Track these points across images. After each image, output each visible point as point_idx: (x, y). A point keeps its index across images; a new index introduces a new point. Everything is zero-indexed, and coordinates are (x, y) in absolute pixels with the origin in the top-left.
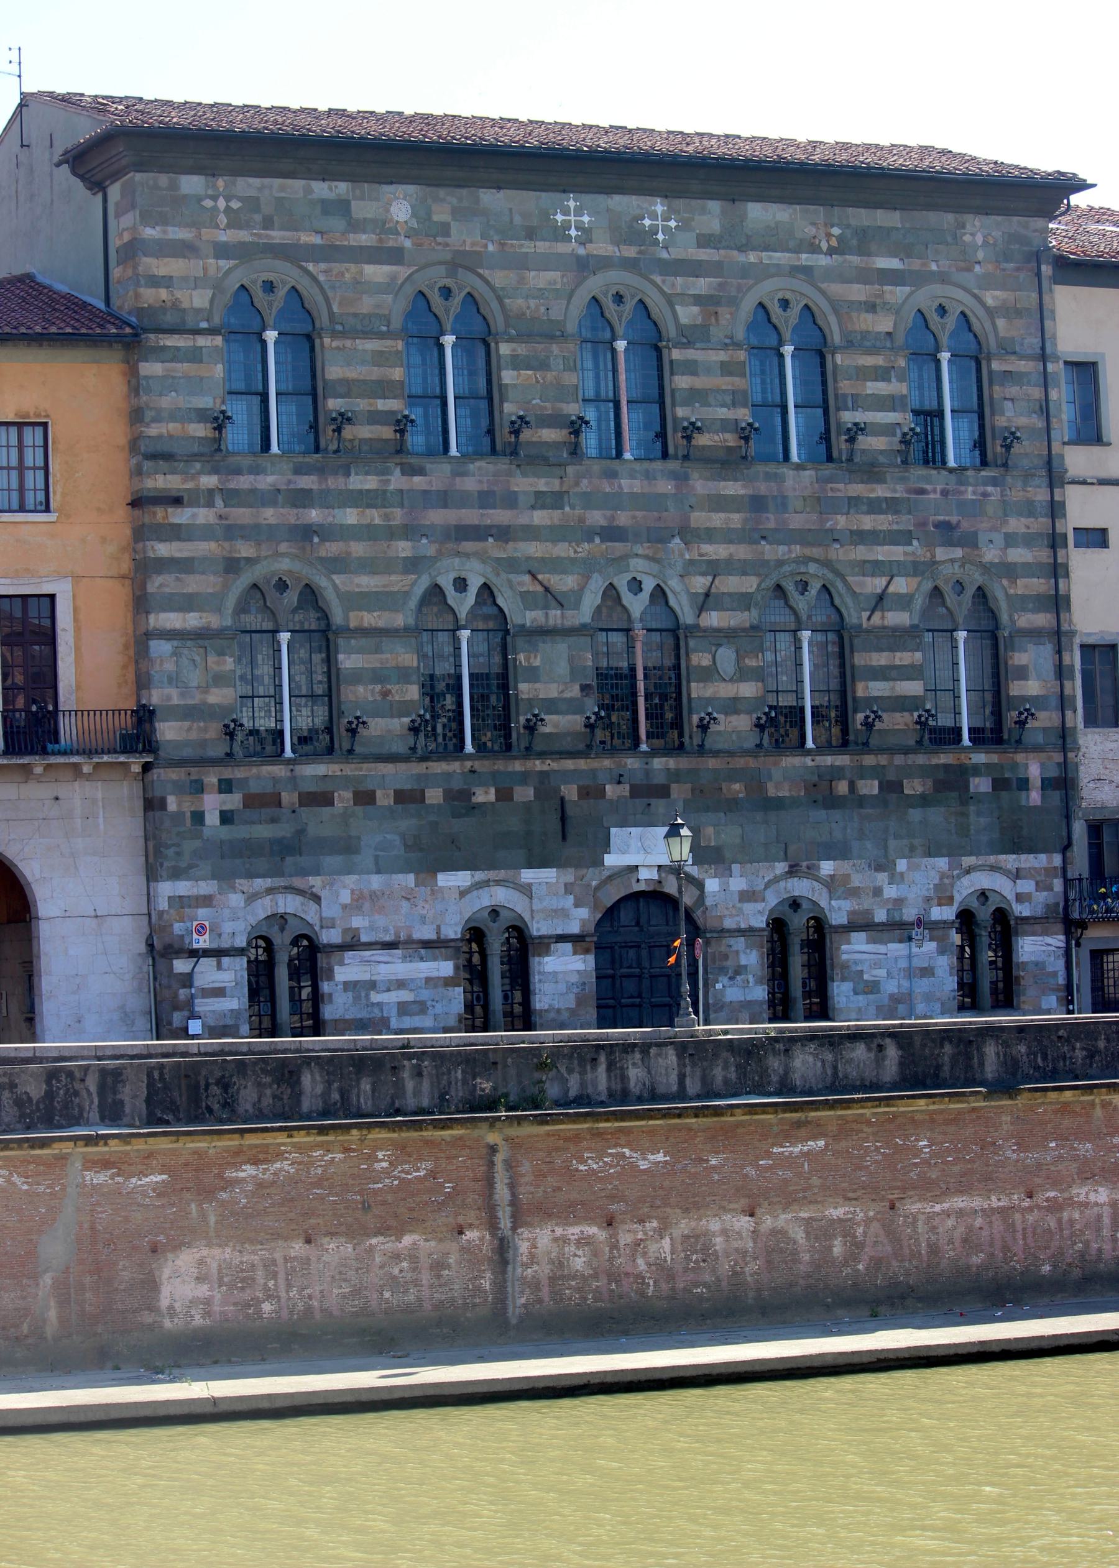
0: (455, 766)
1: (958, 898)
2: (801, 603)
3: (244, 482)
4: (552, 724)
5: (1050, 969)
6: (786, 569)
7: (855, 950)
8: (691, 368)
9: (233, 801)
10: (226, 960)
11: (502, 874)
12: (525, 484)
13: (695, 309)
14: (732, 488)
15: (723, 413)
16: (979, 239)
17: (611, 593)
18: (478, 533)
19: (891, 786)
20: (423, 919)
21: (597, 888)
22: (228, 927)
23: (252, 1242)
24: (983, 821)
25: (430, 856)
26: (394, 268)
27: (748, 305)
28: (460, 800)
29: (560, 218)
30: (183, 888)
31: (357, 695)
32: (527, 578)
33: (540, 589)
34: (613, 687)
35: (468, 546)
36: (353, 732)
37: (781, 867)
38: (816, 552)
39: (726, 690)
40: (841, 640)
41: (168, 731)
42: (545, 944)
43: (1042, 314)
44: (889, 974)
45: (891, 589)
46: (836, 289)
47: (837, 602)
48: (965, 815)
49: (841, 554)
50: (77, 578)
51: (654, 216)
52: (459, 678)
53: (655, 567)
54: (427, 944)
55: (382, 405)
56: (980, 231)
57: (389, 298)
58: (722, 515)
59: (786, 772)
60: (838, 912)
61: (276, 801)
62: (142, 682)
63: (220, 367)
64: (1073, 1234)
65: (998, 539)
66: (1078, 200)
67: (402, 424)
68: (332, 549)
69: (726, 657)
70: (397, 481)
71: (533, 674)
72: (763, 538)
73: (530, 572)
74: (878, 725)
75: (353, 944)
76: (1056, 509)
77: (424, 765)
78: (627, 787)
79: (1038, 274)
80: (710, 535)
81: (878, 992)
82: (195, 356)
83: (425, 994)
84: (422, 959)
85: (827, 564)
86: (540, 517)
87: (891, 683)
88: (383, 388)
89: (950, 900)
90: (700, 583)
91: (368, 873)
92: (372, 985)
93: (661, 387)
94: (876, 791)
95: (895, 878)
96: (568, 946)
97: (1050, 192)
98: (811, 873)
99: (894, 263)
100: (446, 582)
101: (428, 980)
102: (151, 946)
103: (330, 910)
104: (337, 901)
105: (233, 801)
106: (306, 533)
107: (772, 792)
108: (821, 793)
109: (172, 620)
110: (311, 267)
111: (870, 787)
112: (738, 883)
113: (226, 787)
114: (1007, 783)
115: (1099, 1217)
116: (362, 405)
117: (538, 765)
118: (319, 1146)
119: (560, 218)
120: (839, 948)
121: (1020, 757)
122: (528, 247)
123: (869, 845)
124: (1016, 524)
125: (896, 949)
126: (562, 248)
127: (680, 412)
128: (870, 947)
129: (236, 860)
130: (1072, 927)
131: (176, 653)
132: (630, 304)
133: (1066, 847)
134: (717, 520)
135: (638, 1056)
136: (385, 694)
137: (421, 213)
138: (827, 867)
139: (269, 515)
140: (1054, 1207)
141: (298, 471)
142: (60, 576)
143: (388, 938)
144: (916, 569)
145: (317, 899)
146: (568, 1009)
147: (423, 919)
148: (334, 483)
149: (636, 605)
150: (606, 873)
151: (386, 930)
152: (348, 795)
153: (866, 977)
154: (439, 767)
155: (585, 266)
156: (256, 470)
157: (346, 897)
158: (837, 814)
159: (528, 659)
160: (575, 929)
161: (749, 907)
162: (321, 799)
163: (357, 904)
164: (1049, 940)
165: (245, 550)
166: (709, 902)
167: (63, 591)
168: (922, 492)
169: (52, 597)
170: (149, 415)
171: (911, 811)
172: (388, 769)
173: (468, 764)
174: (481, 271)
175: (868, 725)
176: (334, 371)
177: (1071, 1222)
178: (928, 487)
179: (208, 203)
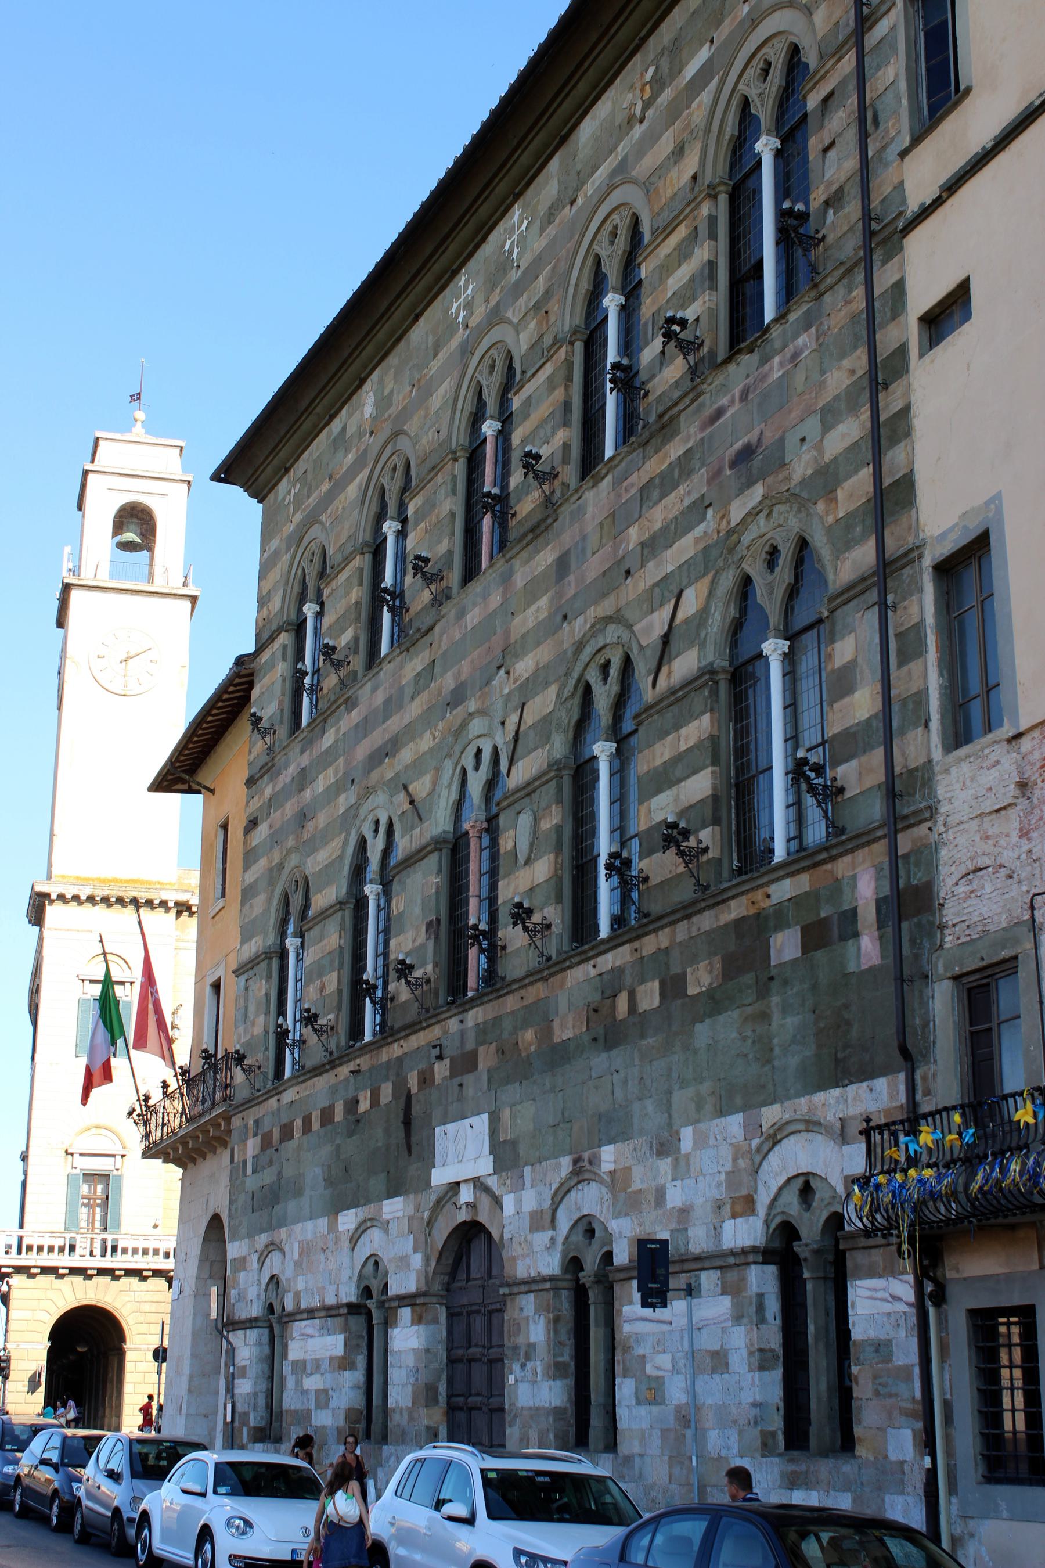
1: (763, 1199)
6: (588, 651)
19: (673, 987)
24: (792, 1021)
37: (566, 1163)
38: (606, 607)
44: (675, 1370)
48: (764, 1016)
77: (335, 1071)
78: (447, 1061)
87: (675, 789)
89: (746, 1205)
94: (656, 1002)
95: (681, 1169)
100: (367, 831)
101: (331, 1358)
111: (649, 996)
123: (650, 1105)
133: (908, 1056)
138: (609, 1156)
146: (408, 1408)
150: (433, 1198)
153: (649, 1369)
158: (618, 1057)
168: (720, 413)
171: (699, 1027)
178: (724, 401)
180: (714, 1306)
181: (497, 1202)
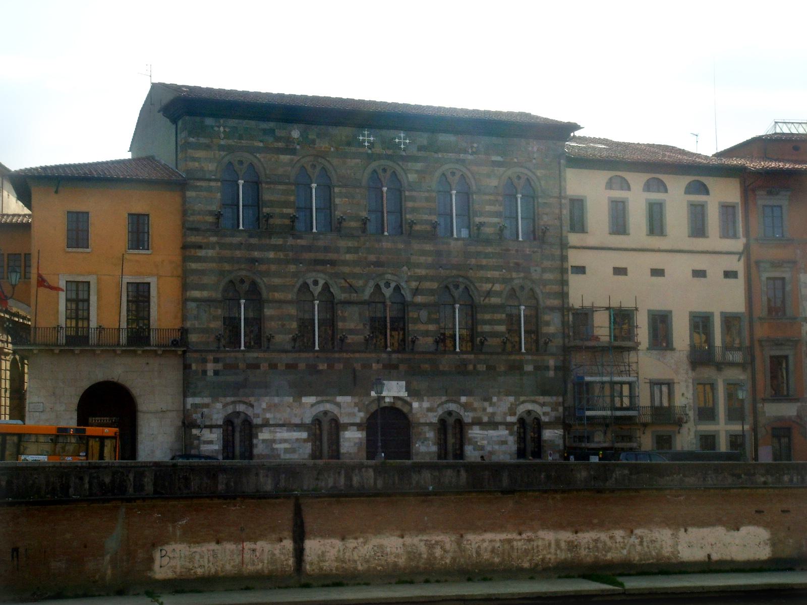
0: (311, 355)
2: (456, 293)
3: (228, 240)
4: (351, 339)
5: (557, 443)
7: (475, 432)
8: (413, 199)
9: (220, 366)
10: (214, 430)
11: (329, 398)
12: (343, 243)
13: (416, 176)
14: (428, 247)
15: (426, 217)
16: (535, 149)
17: (377, 286)
18: (323, 262)
19: (491, 368)
20: (296, 415)
21: (368, 405)
22: (215, 416)
23: (195, 543)
25: (300, 390)
26: (292, 156)
27: (438, 174)
28: (312, 369)
29: (361, 138)
30: (198, 400)
31: (271, 326)
32: (343, 281)
33: (347, 285)
34: (378, 326)
35: (319, 268)
36: (269, 340)
39: (422, 327)
40: (472, 309)
41: (193, 338)
42: (346, 426)
43: (560, 178)
45: (494, 289)
46: (475, 168)
47: (471, 293)
49: (471, 273)
50: (159, 277)
51: (400, 138)
52: (314, 320)
53: (395, 278)
54: (297, 425)
55: (285, 211)
56: (534, 147)
57: (290, 169)
58: (424, 258)
59: (446, 362)
60: (468, 417)
61: (236, 367)
62: (184, 318)
63: (219, 194)
64: (538, 551)
65: (539, 269)
66: (578, 133)
67: (293, 219)
68: (263, 268)
69: (424, 314)
70: (290, 241)
71: (344, 319)
72: (441, 267)
73: (344, 279)
74: (486, 343)
75: (266, 424)
76: (564, 258)
78: (382, 365)
79: (559, 163)
80: (418, 266)
81: (484, 450)
82: (209, 189)
83: (296, 445)
84: (294, 431)
85: (466, 278)
86: (348, 257)
88: (286, 204)
89: (515, 414)
90: (414, 284)
91: (274, 396)
92: (274, 441)
93: (401, 207)
94: (485, 369)
96: (355, 428)
97: (564, 130)
98: (457, 402)
99: (499, 159)
100: (310, 282)
101: (297, 440)
102: (183, 423)
103: (257, 410)
104: (262, 408)
105: (220, 366)
106: (253, 261)
107: (441, 368)
108: (462, 370)
109: (196, 294)
110: (258, 155)
111: (482, 367)
112: (426, 405)
113: (216, 360)
114: (540, 368)
115: (550, 544)
116: (277, 210)
117: (345, 355)
118: (224, 504)
119: (361, 138)
120: (467, 432)
121: (546, 357)
122: (347, 149)
124: (547, 264)
125: (491, 433)
126: (361, 150)
127: (408, 216)
128: (481, 432)
129: (218, 391)
130: (567, 427)
131: (198, 307)
132: (389, 173)
133: (564, 394)
134: (422, 259)
135: (357, 471)
136: (283, 325)
137: (304, 134)
138: (463, 399)
139: (238, 253)
140: (530, 540)
141: (251, 236)
142: (151, 275)
143: (281, 422)
144: (505, 281)
145: (252, 406)
147: (296, 415)
148: (266, 241)
149: (388, 292)
151: (280, 419)
152: (266, 365)
153: (479, 444)
154: (304, 355)
155: (370, 158)
156: (233, 236)
157: (264, 405)
159: (342, 313)
160: (358, 421)
161: (430, 414)
162: (256, 366)
163: (270, 408)
164: (556, 431)
165: (227, 267)
166: (414, 412)
167: (153, 281)
169: (149, 284)
170: (189, 212)
172: (284, 356)
173: (316, 354)
174: (328, 159)
175: (482, 343)
176: (267, 196)
177: (538, 546)
179: (216, 129)
180: (503, 432)
181: (411, 405)
